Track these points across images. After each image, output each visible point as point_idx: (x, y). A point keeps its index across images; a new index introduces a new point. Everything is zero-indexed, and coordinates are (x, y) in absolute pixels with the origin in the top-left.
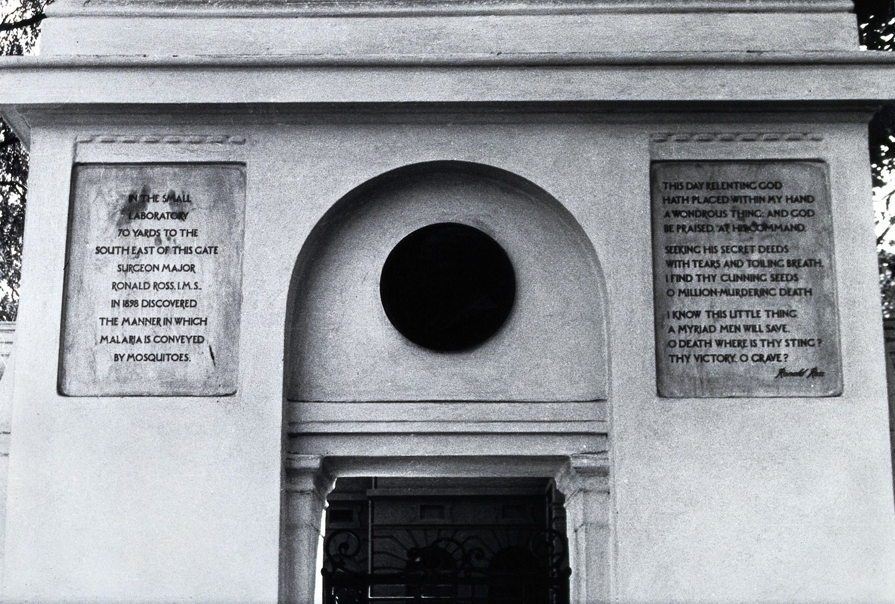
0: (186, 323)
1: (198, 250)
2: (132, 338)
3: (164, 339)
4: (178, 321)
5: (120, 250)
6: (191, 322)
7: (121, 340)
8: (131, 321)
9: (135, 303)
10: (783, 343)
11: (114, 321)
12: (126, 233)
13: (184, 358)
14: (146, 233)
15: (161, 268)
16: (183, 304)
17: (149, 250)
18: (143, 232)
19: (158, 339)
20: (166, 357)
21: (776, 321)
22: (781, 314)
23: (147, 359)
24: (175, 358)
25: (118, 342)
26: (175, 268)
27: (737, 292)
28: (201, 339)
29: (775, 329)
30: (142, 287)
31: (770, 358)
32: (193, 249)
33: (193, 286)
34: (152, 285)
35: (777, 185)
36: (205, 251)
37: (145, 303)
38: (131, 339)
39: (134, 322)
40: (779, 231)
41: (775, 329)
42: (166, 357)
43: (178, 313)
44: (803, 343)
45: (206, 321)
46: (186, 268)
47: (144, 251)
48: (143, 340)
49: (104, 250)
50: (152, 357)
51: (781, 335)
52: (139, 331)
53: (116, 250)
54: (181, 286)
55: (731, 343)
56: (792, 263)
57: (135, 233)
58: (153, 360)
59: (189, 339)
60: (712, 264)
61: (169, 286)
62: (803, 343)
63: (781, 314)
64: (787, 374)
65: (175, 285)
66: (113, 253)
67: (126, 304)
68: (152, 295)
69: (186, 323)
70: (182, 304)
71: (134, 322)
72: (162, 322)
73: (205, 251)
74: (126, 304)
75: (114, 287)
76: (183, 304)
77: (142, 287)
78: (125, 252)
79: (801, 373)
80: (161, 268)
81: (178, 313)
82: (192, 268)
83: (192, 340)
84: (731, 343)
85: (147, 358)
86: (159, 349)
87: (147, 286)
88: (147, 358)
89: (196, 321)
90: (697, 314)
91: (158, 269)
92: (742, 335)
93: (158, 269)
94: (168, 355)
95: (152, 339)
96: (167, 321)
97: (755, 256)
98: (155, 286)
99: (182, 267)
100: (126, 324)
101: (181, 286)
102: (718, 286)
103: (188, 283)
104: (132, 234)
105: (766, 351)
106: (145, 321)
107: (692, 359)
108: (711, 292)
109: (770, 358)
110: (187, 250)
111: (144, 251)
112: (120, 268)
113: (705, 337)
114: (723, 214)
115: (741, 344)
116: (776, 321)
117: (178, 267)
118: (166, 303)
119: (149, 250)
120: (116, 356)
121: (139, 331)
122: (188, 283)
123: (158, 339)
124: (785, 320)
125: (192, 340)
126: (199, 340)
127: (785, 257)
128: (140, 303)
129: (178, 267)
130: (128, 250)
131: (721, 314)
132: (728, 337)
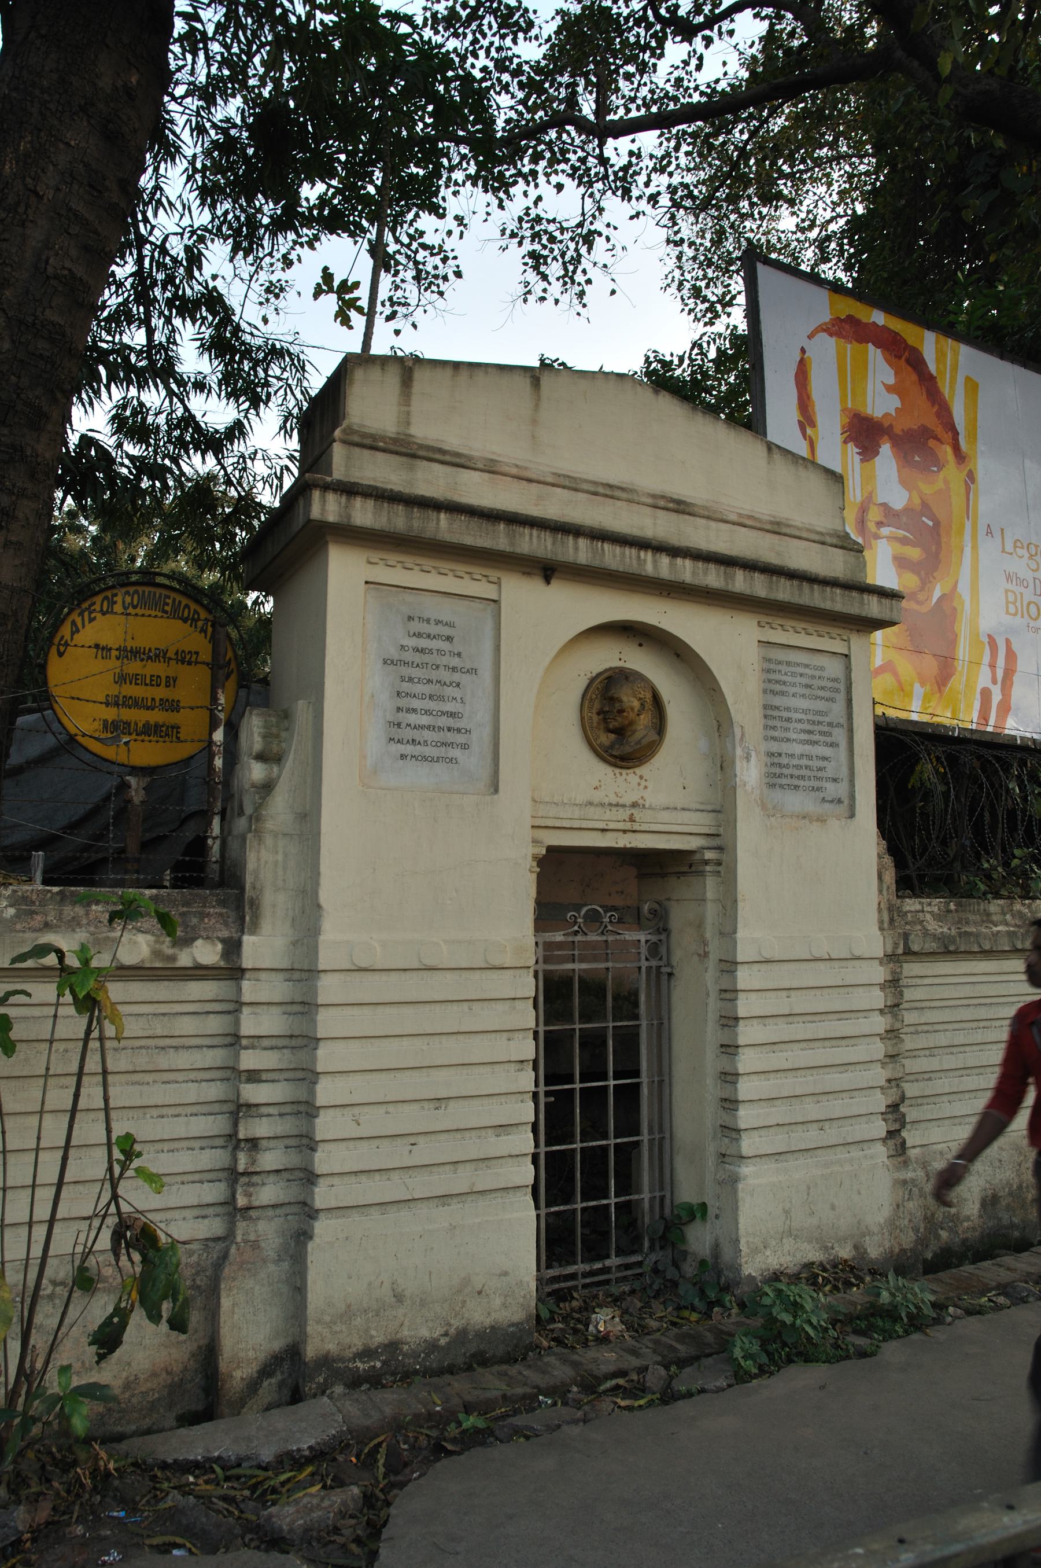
6: (459, 730)
9: (414, 710)
11: (399, 725)
21: (821, 764)
31: (818, 789)
35: (822, 669)
41: (820, 769)
55: (798, 777)
56: (830, 724)
60: (788, 720)
63: (825, 759)
76: (452, 715)
79: (832, 801)
82: (458, 685)
84: (798, 777)
85: (425, 759)
88: (425, 759)
90: (780, 755)
92: (803, 772)
106: (422, 727)
108: (788, 740)
109: (818, 789)
113: (785, 771)
114: (794, 685)
115: (803, 777)
116: (821, 764)
124: (825, 763)
127: (827, 719)
132: (796, 772)
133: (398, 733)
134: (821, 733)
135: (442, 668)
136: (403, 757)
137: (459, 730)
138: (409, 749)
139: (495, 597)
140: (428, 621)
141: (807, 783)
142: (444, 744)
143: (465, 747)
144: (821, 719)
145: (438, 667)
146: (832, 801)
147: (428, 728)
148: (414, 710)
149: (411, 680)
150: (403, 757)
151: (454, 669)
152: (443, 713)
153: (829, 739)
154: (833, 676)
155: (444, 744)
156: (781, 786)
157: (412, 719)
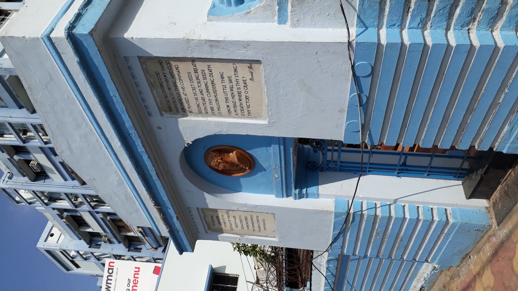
10: (237, 78)
21: (226, 79)
22: (222, 77)
27: (215, 92)
29: (230, 81)
40: (180, 75)
41: (230, 81)
44: (235, 70)
51: (233, 79)
62: (235, 70)
63: (222, 77)
64: (252, 78)
79: (252, 73)
84: (240, 96)
90: (228, 106)
97: (196, 85)
102: (213, 99)
105: (242, 84)
106: (253, 224)
107: (249, 109)
115: (239, 93)
116: (226, 79)
124: (225, 76)
131: (227, 99)
132: (237, 98)
133: (257, 228)
134: (205, 78)
141: (243, 90)
144: (194, 78)
146: (252, 73)
153: (207, 72)
154: (160, 67)
156: (248, 107)
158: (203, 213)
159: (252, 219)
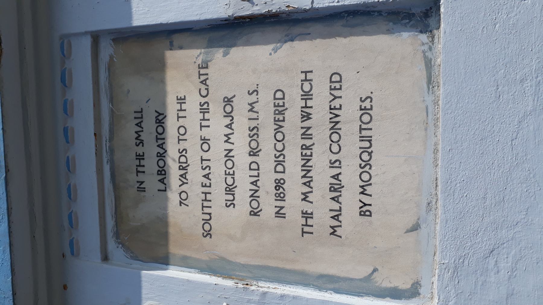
0: (309, 103)
1: (204, 93)
2: (332, 189)
3: (335, 137)
4: (306, 117)
5: (206, 204)
6: (307, 96)
7: (336, 206)
8: (306, 189)
9: (279, 184)
11: (307, 215)
12: (184, 196)
13: (367, 104)
14: (184, 169)
15: (229, 146)
16: (280, 110)
17: (205, 164)
18: (183, 172)
19: (335, 148)
20: (364, 133)
23: (368, 163)
24: (366, 118)
25: (340, 210)
26: (229, 126)
28: (336, 78)
30: (255, 173)
32: (203, 100)
33: (253, 98)
34: (254, 159)
36: (204, 82)
37: (280, 168)
38: (335, 190)
39: (307, 184)
42: (364, 133)
43: (293, 115)
45: (306, 72)
46: (228, 109)
47: (207, 171)
48: (335, 171)
49: (207, 227)
50: (365, 157)
52: (322, 176)
53: (207, 210)
54: (255, 116)
57: (184, 183)
58: (370, 154)
59: (335, 98)
61: (254, 133)
65: (253, 124)
66: (210, 214)
67: (280, 197)
68: (267, 161)
69: (309, 103)
70: (280, 113)
71: (307, 184)
72: (308, 143)
73: (204, 82)
74: (280, 197)
75: (255, 214)
76: (280, 110)
77: (255, 173)
78: (209, 197)
80: (229, 146)
81: (293, 115)
82: (228, 101)
83: (336, 93)
85: (365, 165)
86: (351, 145)
87: (254, 166)
88: (365, 165)
89: (307, 87)
91: (230, 151)
93: (230, 151)
94: (361, 129)
95: (334, 158)
96: (306, 135)
98: (254, 155)
99: (228, 115)
100: (311, 198)
101: (255, 116)
103: (250, 104)
104: (184, 188)
106: (306, 169)
110: (204, 110)
111: (207, 171)
112: (230, 204)
117: (227, 121)
118: (279, 136)
119: (205, 164)
120: (362, 214)
121: (322, 176)
122: (250, 104)
123: (335, 148)
125: (336, 93)
126: (336, 82)
128: (279, 176)
129: (227, 121)
130: (206, 193)
135: (205, 132)
136: (365, 211)
137: (307, 96)
138: (350, 199)
139: (87, 42)
140: (140, 157)
142: (335, 127)
143: (336, 82)
145: (205, 141)
147: (307, 158)
148: (279, 184)
149: (230, 190)
150: (365, 211)
151: (204, 110)
152: (279, 129)
155: (335, 127)
157: (294, 187)
158: (111, 100)
159: (306, 117)
